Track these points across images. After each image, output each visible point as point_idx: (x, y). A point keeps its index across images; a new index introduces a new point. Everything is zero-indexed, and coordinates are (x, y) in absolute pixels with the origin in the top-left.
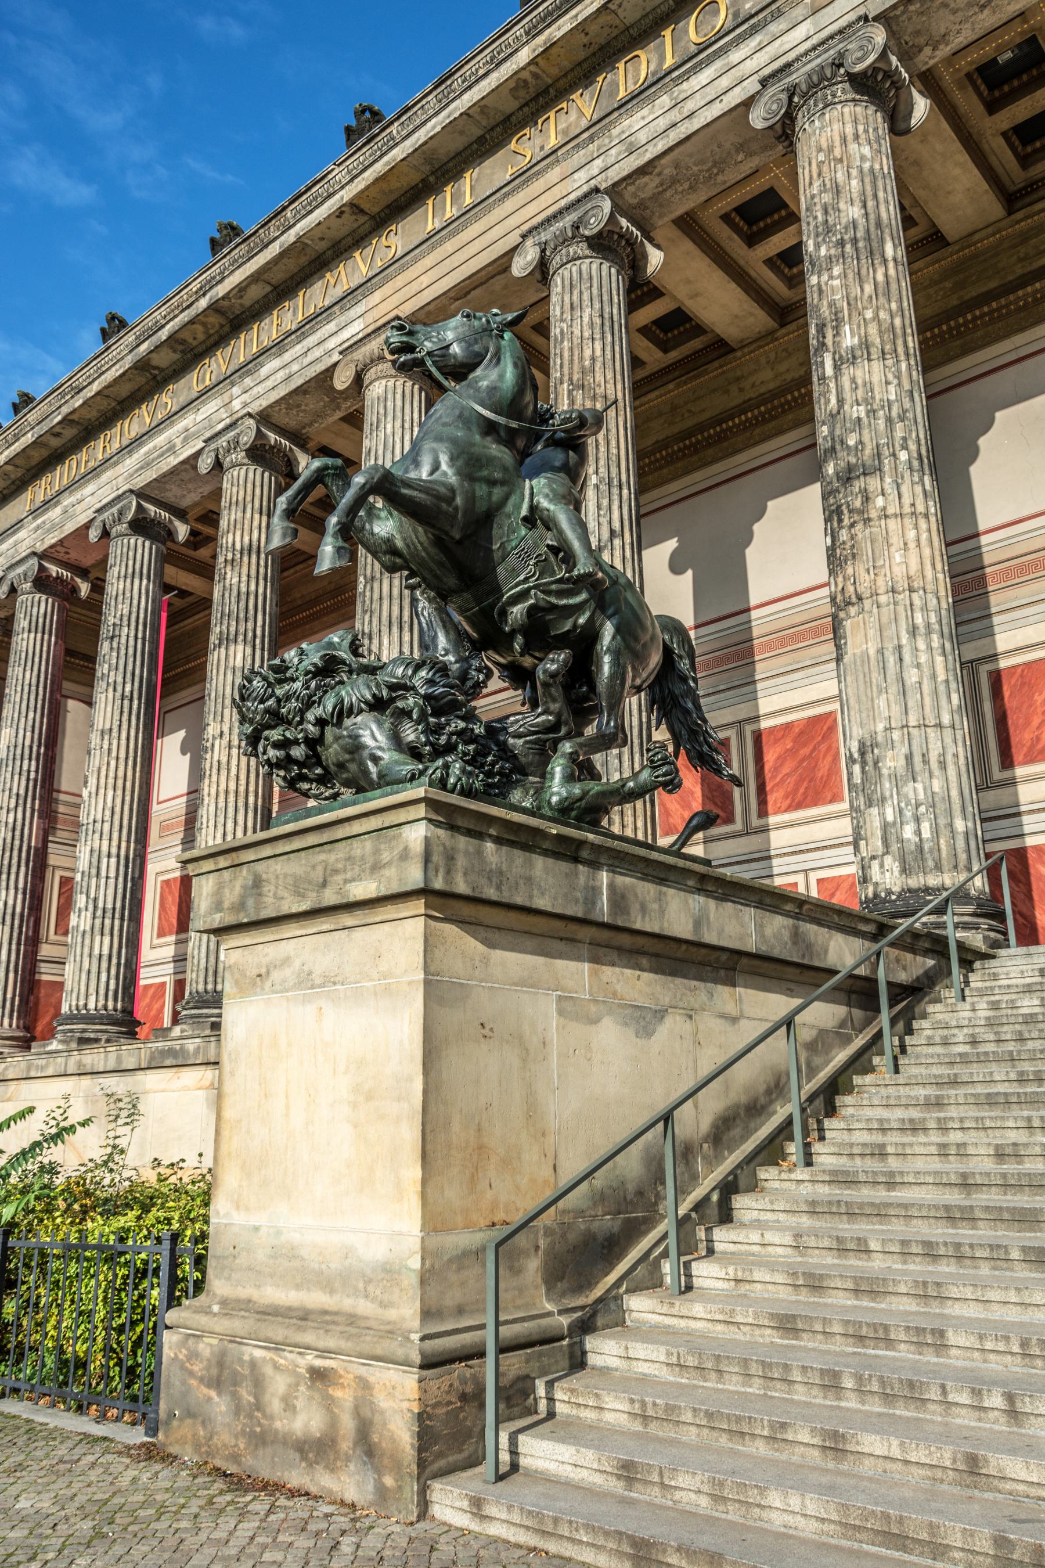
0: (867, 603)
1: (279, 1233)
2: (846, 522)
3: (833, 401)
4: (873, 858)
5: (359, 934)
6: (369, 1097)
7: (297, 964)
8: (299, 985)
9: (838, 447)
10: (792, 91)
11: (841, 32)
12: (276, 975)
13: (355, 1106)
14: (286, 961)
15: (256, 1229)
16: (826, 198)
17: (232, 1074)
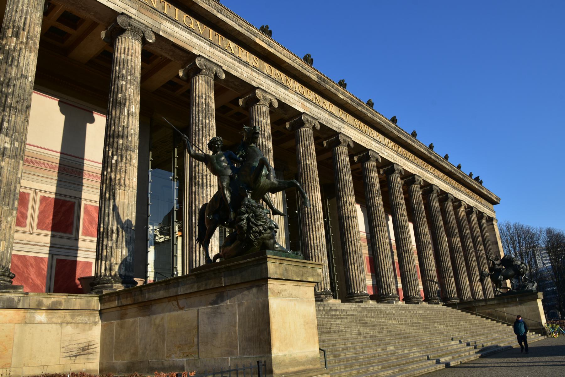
0: (127, 188)
1: (291, 355)
2: (124, 160)
3: (126, 123)
4: (116, 264)
5: (302, 288)
6: (307, 324)
7: (288, 291)
8: (289, 297)
9: (125, 138)
10: (130, 25)
11: (146, 26)
12: (283, 293)
13: (305, 325)
14: (285, 290)
15: (285, 355)
16: (133, 64)
17: (274, 317)
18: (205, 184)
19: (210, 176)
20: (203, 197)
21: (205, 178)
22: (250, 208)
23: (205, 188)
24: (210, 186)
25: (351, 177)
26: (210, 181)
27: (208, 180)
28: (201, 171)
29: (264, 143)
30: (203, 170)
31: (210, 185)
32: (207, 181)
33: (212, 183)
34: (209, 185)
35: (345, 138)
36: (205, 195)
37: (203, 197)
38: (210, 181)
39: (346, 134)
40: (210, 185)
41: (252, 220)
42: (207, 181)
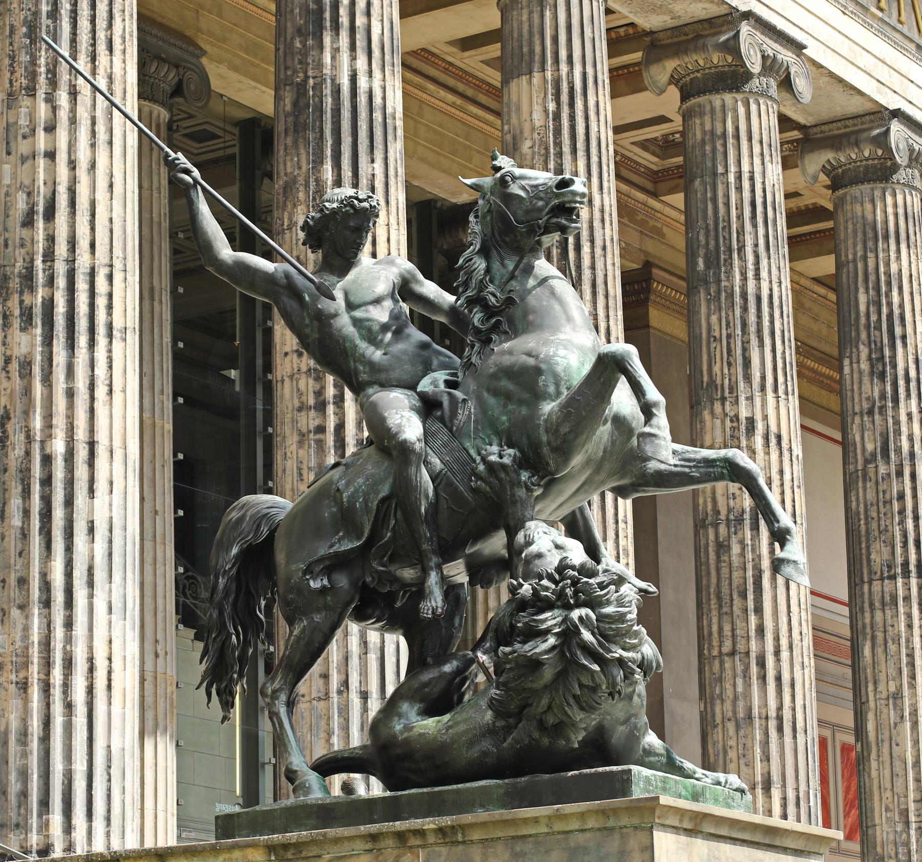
18: (82, 324)
19: (110, 277)
20: (70, 394)
21: (82, 286)
22: (575, 582)
23: (82, 340)
24: (110, 336)
25: (786, 283)
26: (110, 307)
27: (101, 302)
28: (61, 249)
29: (363, 83)
30: (72, 243)
31: (110, 327)
32: (92, 306)
33: (118, 323)
34: (101, 330)
35: (772, 47)
36: (81, 384)
37: (70, 394)
38: (110, 307)
39: (781, 25)
40: (110, 327)
41: (587, 636)
42: (92, 306)
